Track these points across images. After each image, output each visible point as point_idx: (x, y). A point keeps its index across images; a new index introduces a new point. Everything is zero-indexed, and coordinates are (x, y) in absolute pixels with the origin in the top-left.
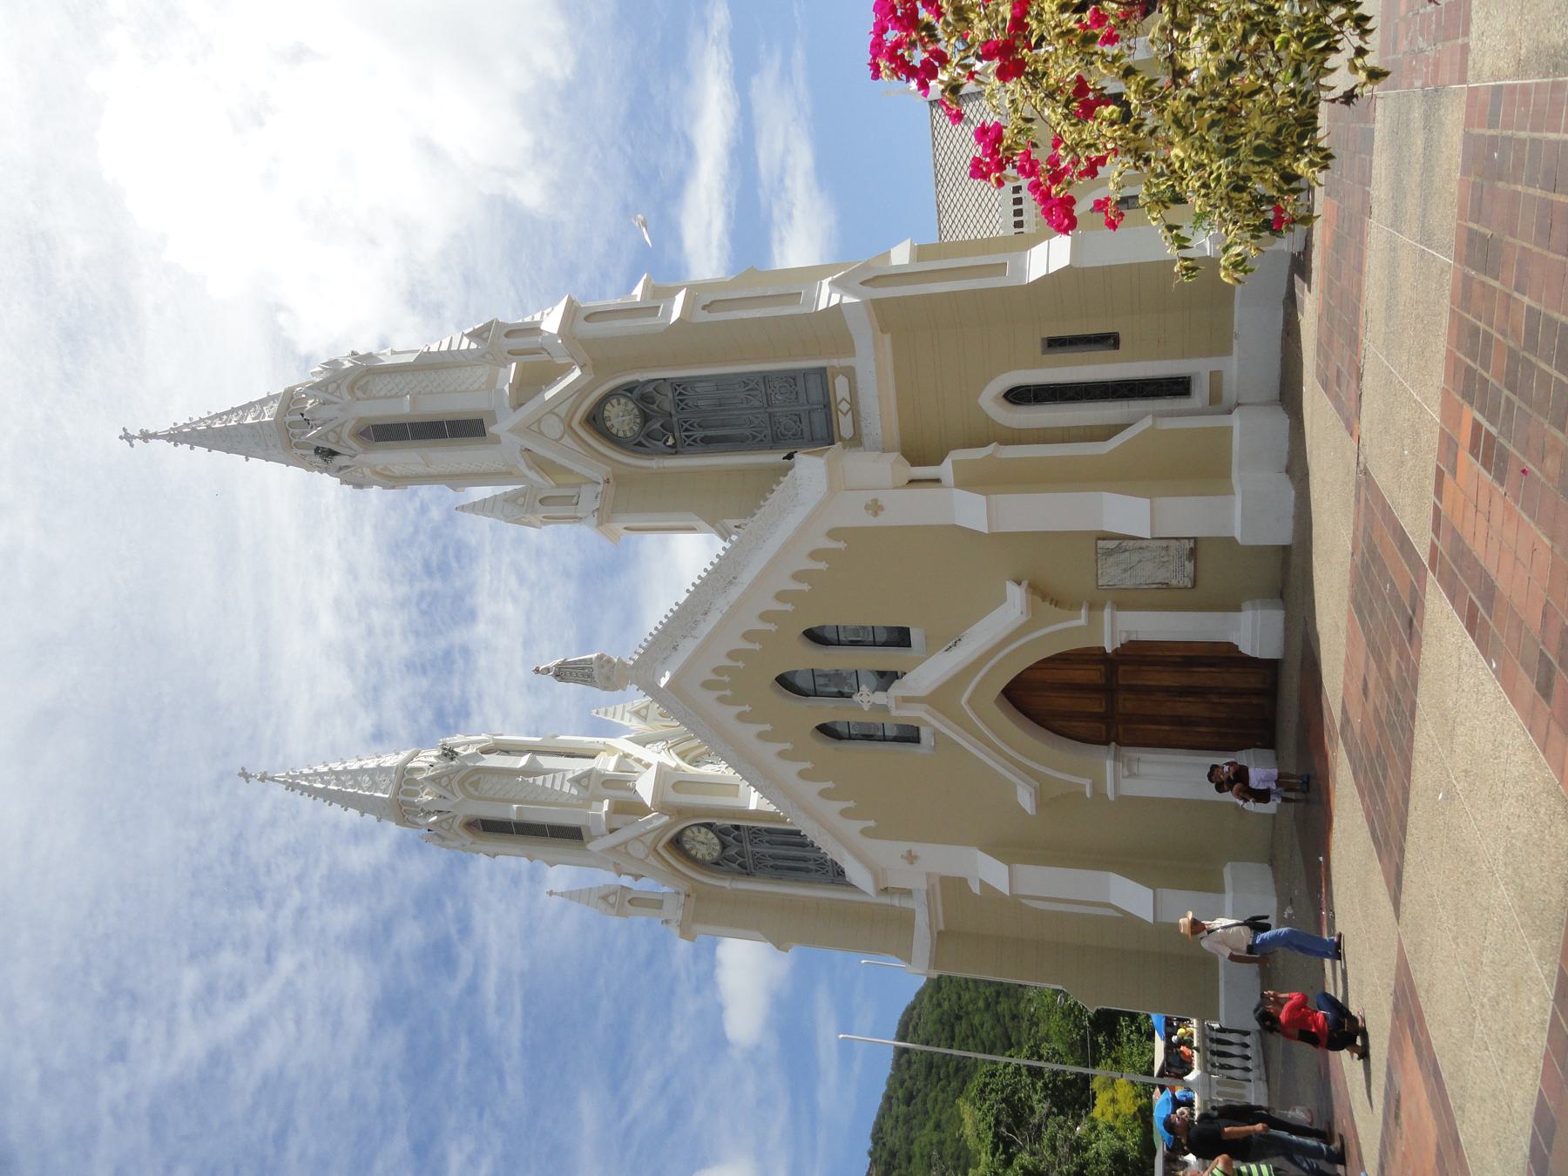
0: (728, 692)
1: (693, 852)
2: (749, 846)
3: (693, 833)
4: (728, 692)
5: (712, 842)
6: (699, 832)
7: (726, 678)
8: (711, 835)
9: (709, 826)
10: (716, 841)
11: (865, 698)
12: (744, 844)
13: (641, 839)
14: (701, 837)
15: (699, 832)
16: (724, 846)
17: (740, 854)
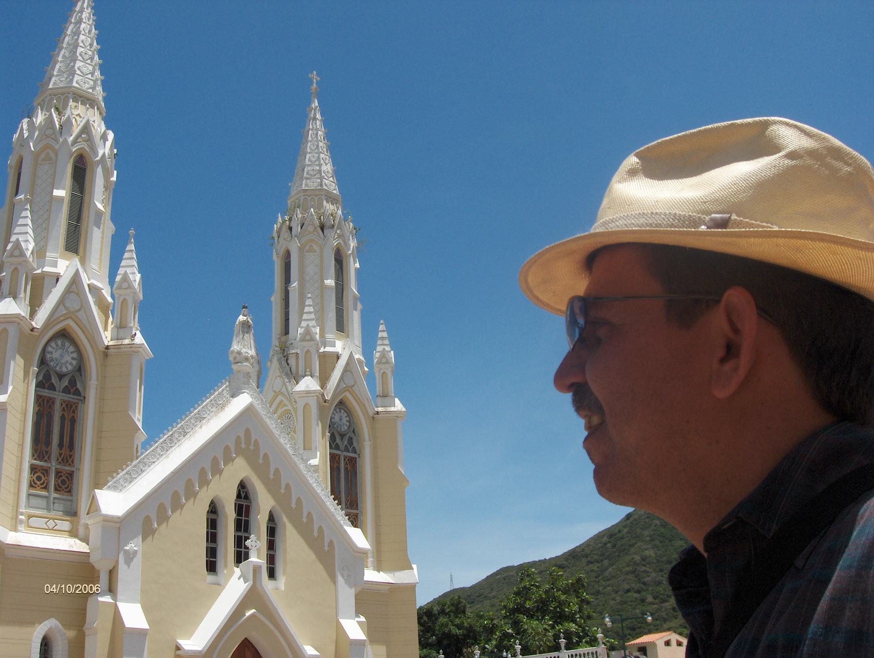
0: (243, 446)
1: (53, 344)
2: (62, 398)
3: (72, 353)
4: (243, 446)
5: (64, 366)
6: (73, 358)
7: (252, 447)
8: (70, 368)
9: (80, 369)
10: (64, 370)
11: (254, 544)
12: (61, 394)
13: (83, 310)
14: (68, 358)
15: (73, 358)
16: (61, 376)
17: (52, 388)
